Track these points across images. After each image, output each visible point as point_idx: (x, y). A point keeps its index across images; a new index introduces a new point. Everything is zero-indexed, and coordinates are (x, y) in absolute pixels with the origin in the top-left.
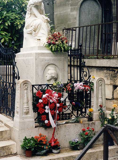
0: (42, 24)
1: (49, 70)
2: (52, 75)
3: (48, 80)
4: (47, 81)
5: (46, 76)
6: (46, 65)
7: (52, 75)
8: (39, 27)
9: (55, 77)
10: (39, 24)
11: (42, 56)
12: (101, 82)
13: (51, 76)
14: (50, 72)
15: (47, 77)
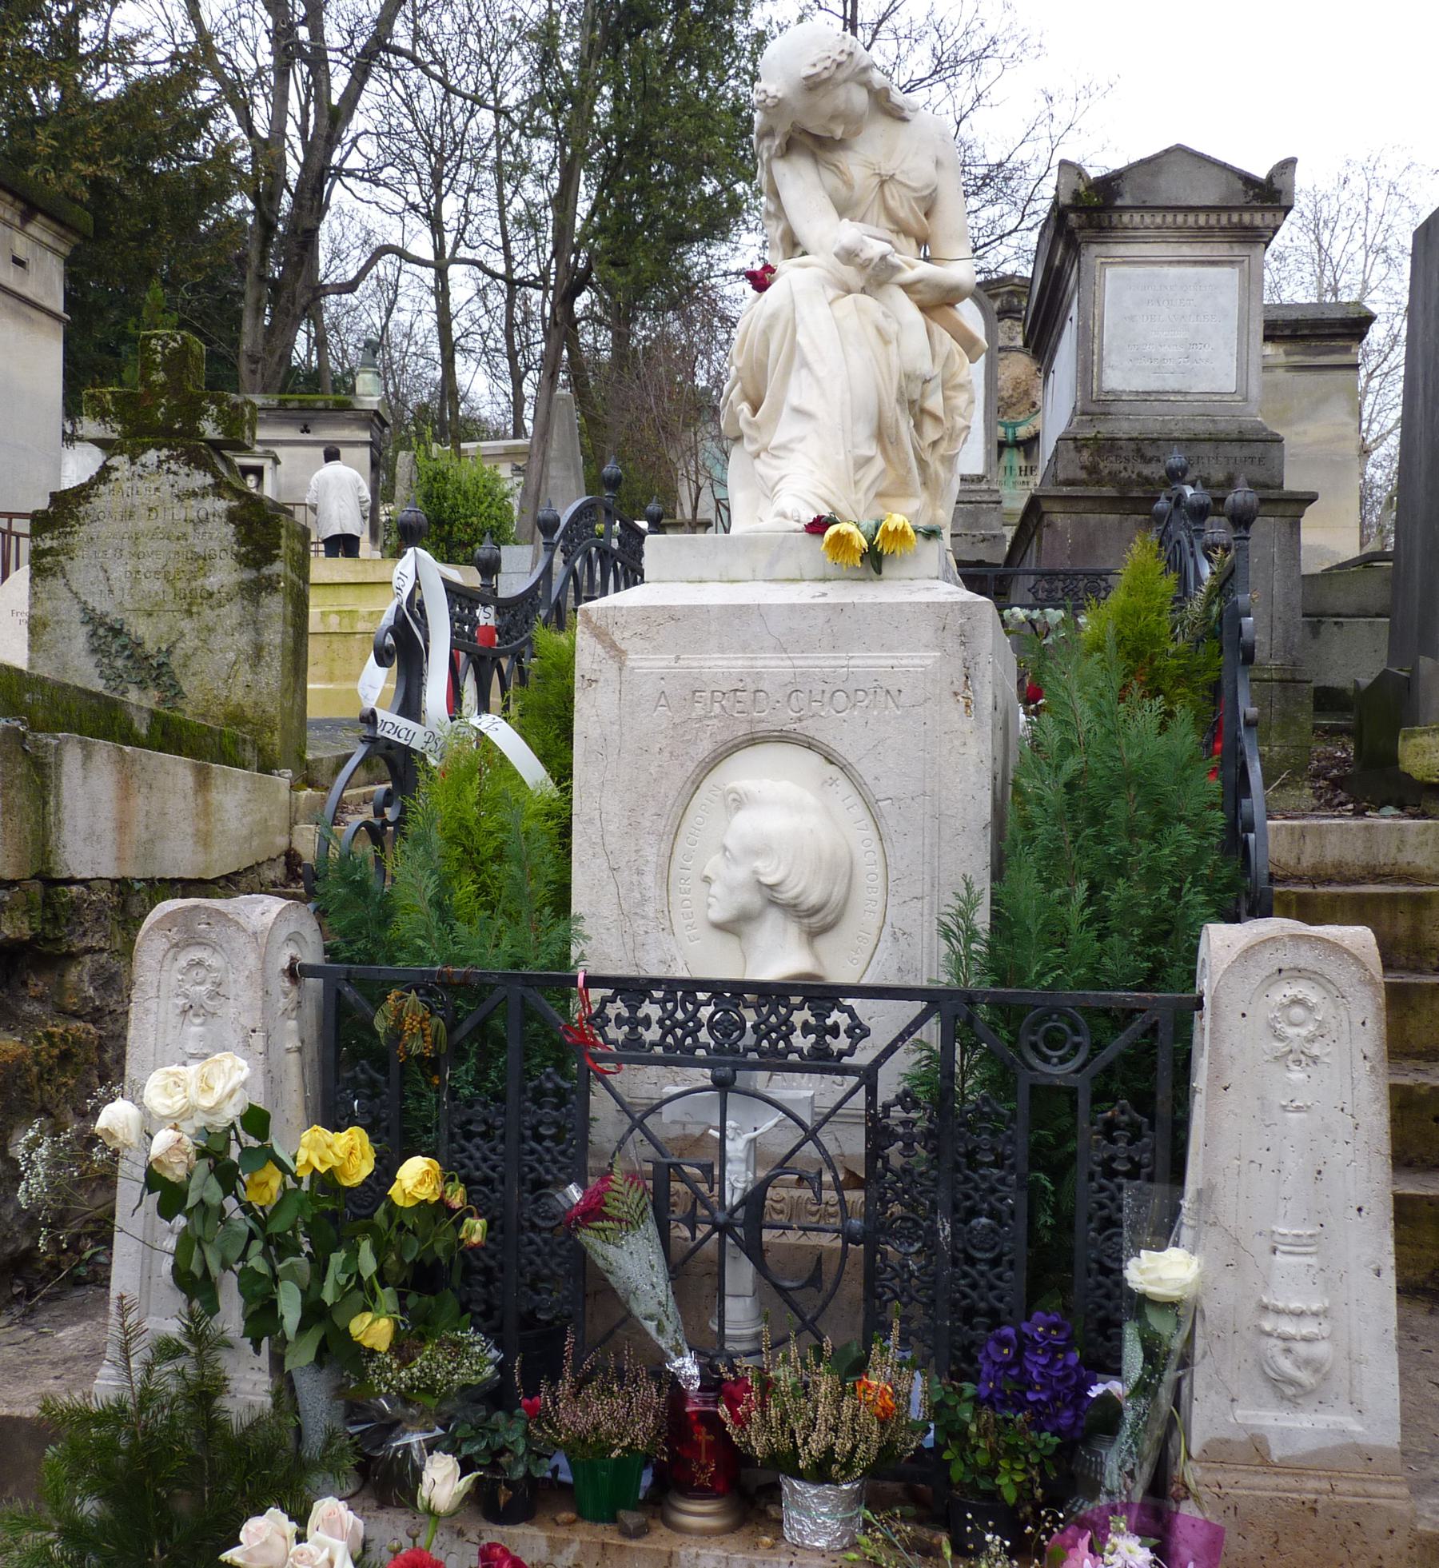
0: (803, 310)
1: (739, 802)
2: (759, 864)
3: (720, 927)
4: (717, 937)
5: (707, 872)
6: (704, 748)
7: (759, 864)
8: (773, 347)
9: (787, 894)
10: (774, 317)
11: (657, 649)
12: (1297, 1002)
13: (741, 874)
14: (746, 824)
15: (716, 889)
